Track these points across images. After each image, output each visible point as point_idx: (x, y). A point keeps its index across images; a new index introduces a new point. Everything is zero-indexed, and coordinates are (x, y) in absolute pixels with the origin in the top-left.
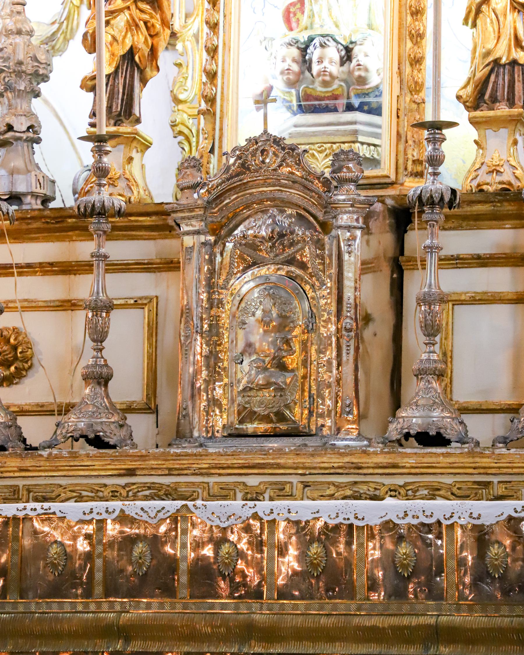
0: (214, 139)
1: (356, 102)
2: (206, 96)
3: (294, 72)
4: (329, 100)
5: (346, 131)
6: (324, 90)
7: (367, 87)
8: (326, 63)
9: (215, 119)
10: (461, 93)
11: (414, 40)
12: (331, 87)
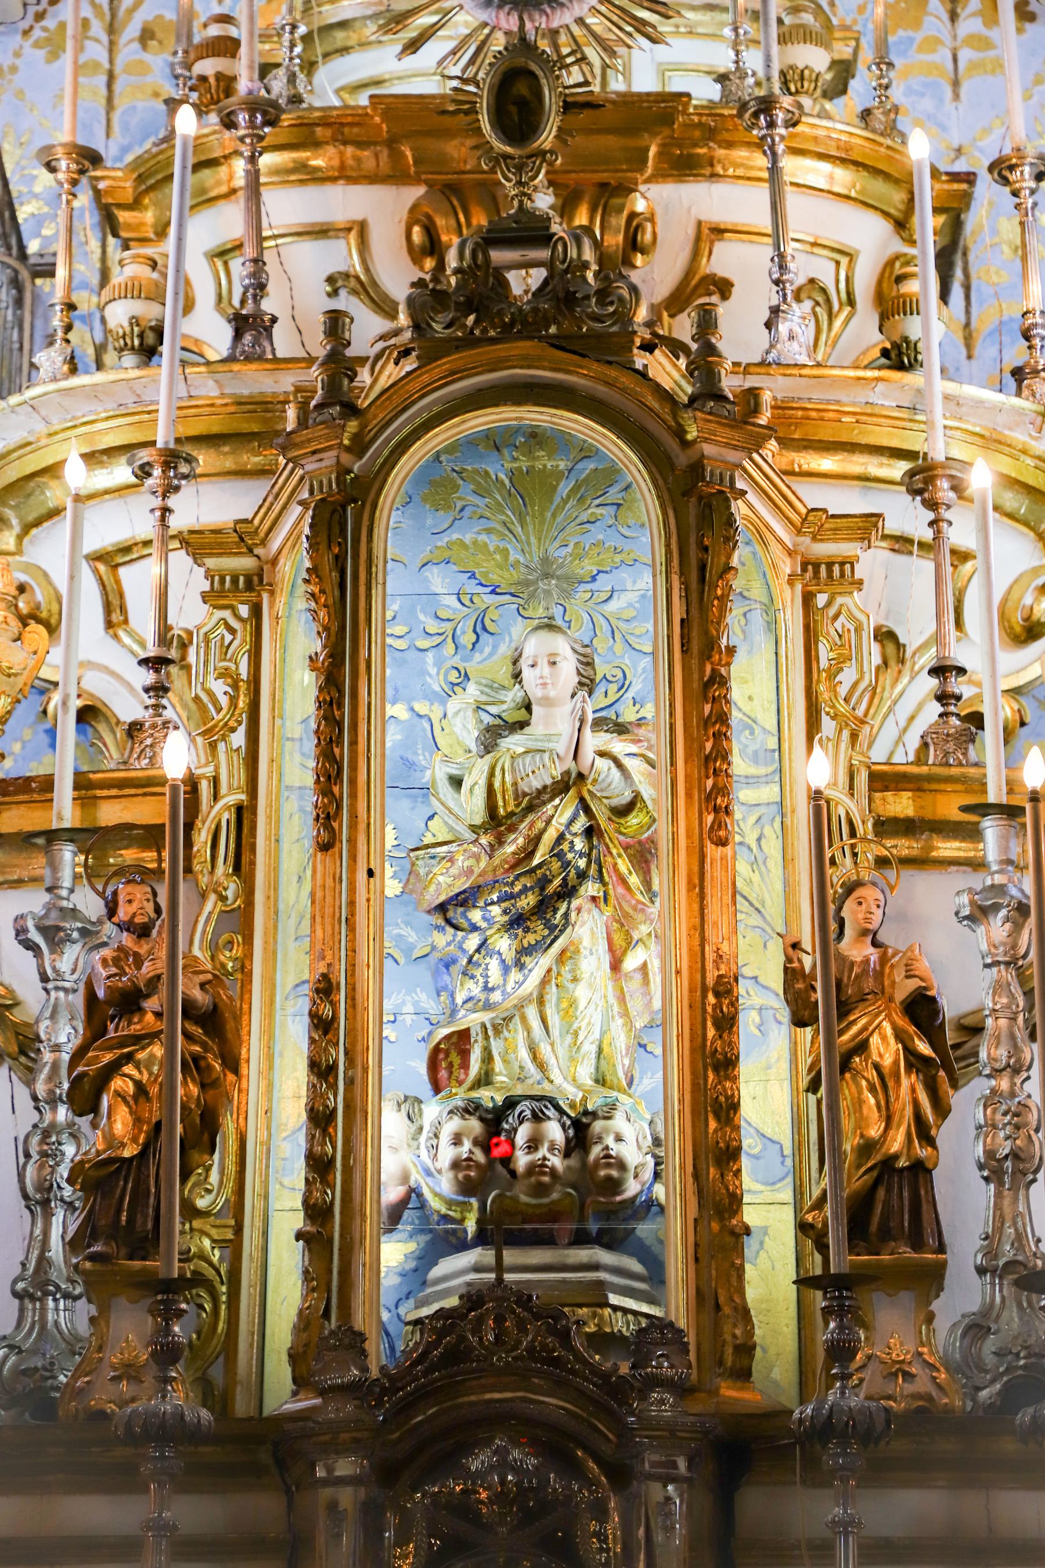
0: (329, 1291)
1: (593, 1227)
2: (315, 1205)
3: (478, 1165)
4: (542, 1222)
5: (581, 1282)
6: (533, 1201)
7: (618, 1198)
8: (543, 1151)
9: (332, 1251)
10: (809, 1218)
11: (723, 1114)
12: (548, 1196)
